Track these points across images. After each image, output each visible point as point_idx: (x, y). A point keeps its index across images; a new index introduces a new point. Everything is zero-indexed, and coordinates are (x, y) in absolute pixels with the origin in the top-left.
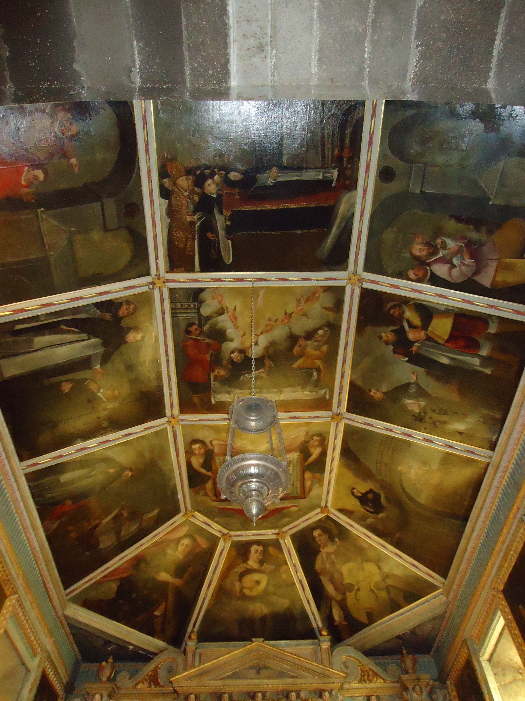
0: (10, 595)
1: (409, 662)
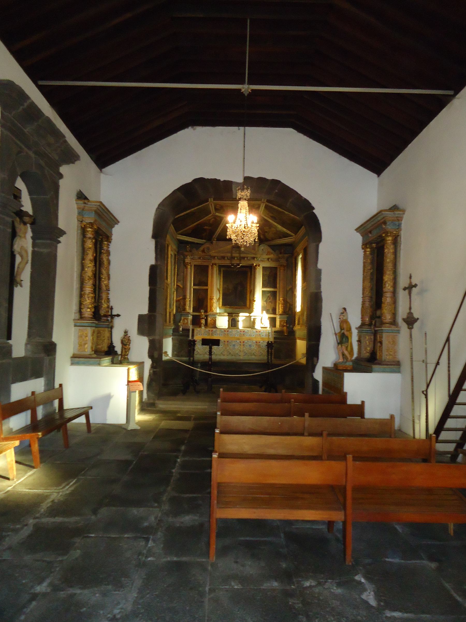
1: (282, 251)
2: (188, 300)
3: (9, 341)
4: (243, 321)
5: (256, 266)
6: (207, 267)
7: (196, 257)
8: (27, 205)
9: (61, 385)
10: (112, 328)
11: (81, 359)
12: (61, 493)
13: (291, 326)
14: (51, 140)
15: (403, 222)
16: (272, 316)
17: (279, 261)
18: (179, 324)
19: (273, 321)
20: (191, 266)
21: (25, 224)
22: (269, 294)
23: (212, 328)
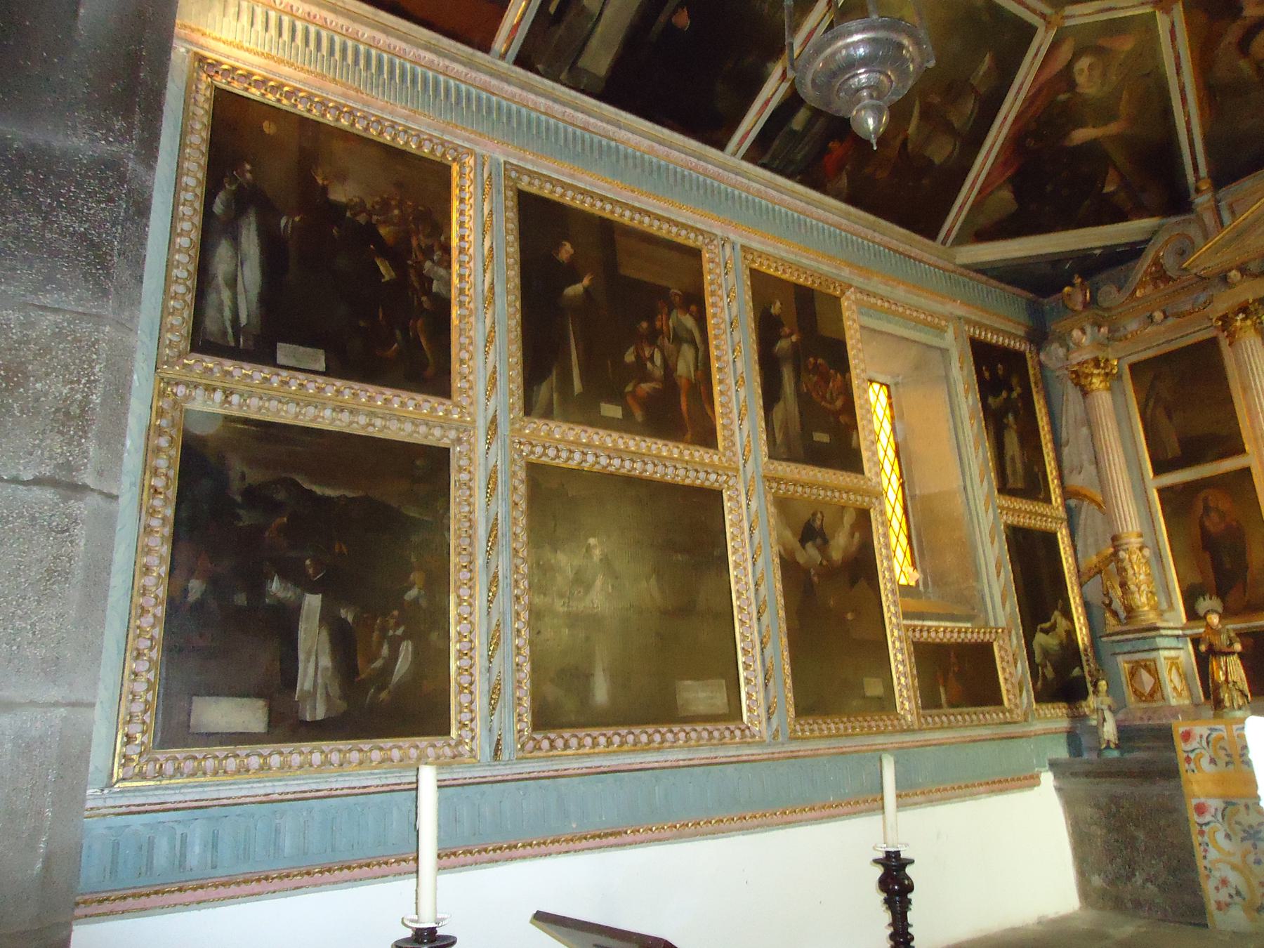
0: (843, 293)
6: (1213, 342)
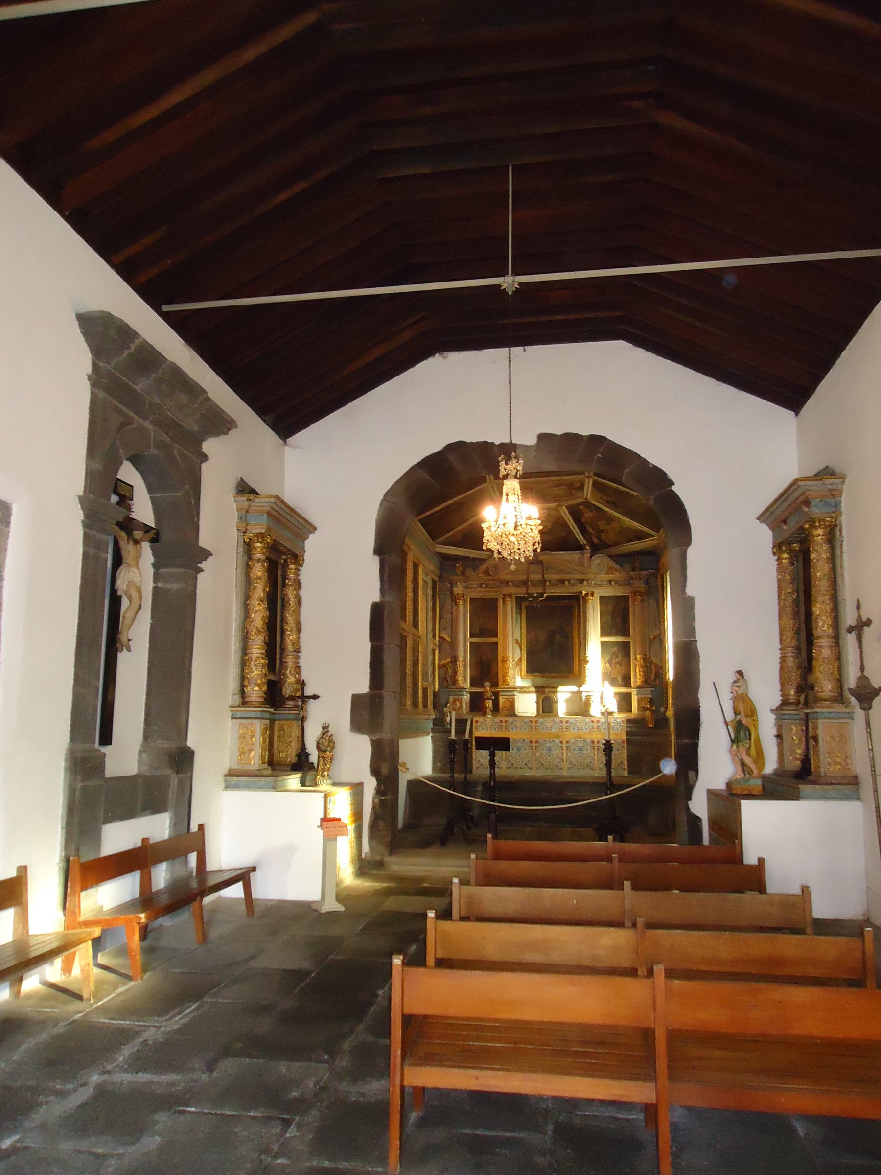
2: (460, 664)
3: (105, 749)
4: (567, 701)
5: (587, 595)
6: (495, 601)
7: (474, 583)
8: (143, 510)
9: (201, 827)
10: (303, 719)
11: (241, 779)
12: (162, 1029)
13: (662, 709)
14: (183, 398)
15: (843, 498)
16: (623, 690)
17: (629, 584)
18: (445, 710)
19: (625, 702)
20: (465, 601)
21: (137, 542)
22: (615, 649)
23: (507, 716)
